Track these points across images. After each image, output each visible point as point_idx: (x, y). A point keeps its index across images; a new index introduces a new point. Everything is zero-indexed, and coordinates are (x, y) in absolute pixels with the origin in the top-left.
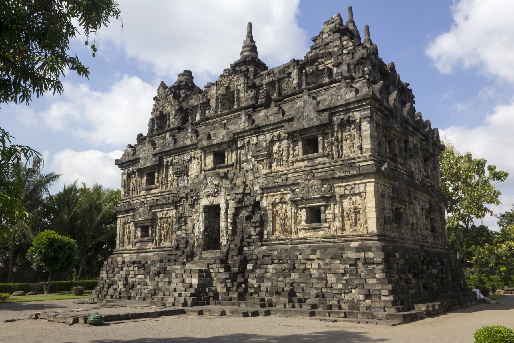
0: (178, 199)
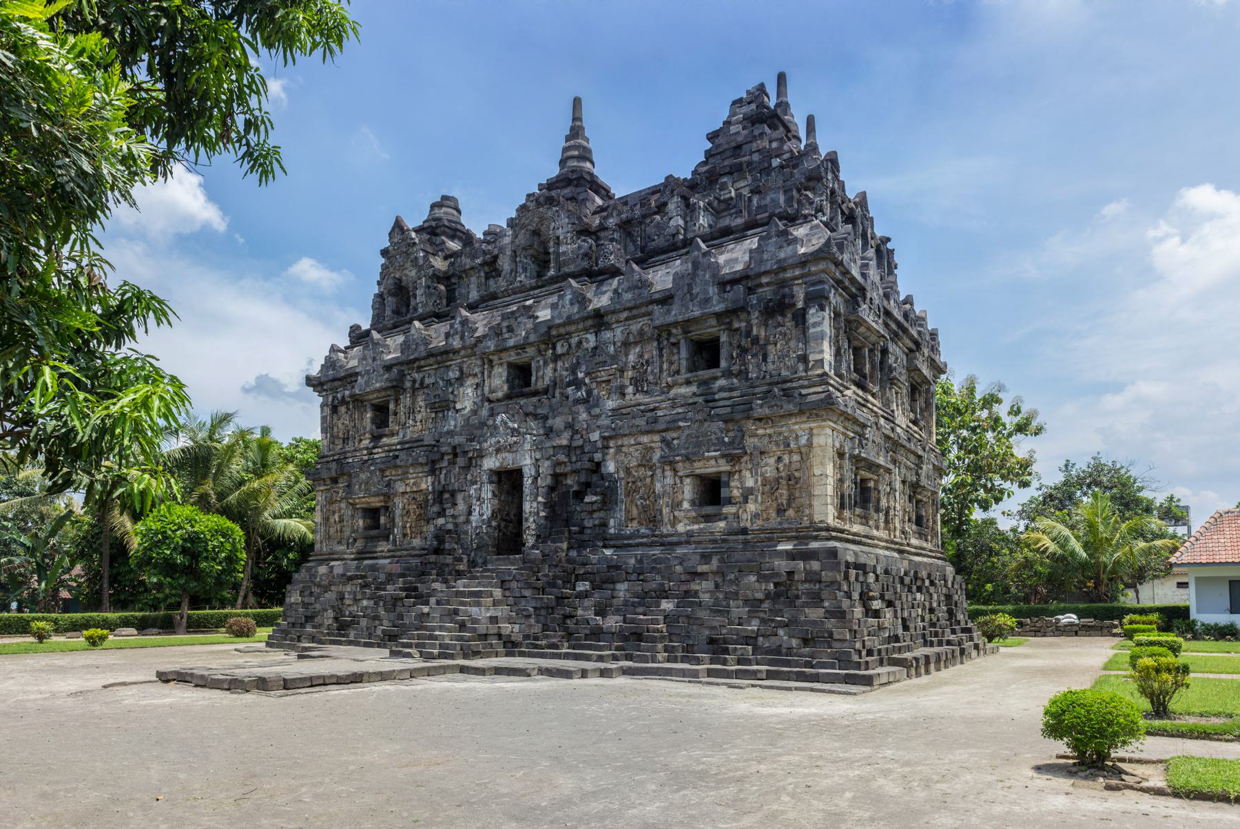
0: (437, 457)
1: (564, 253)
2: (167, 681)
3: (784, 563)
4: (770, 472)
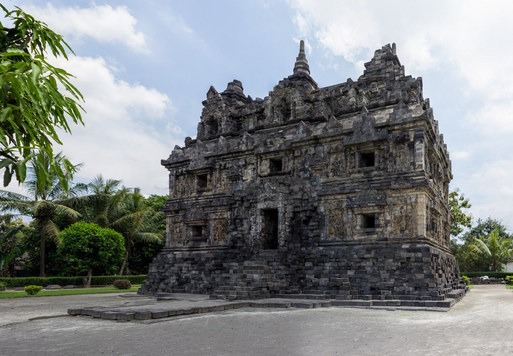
0: (233, 202)
1: (298, 110)
2: (75, 315)
3: (406, 254)
4: (397, 213)
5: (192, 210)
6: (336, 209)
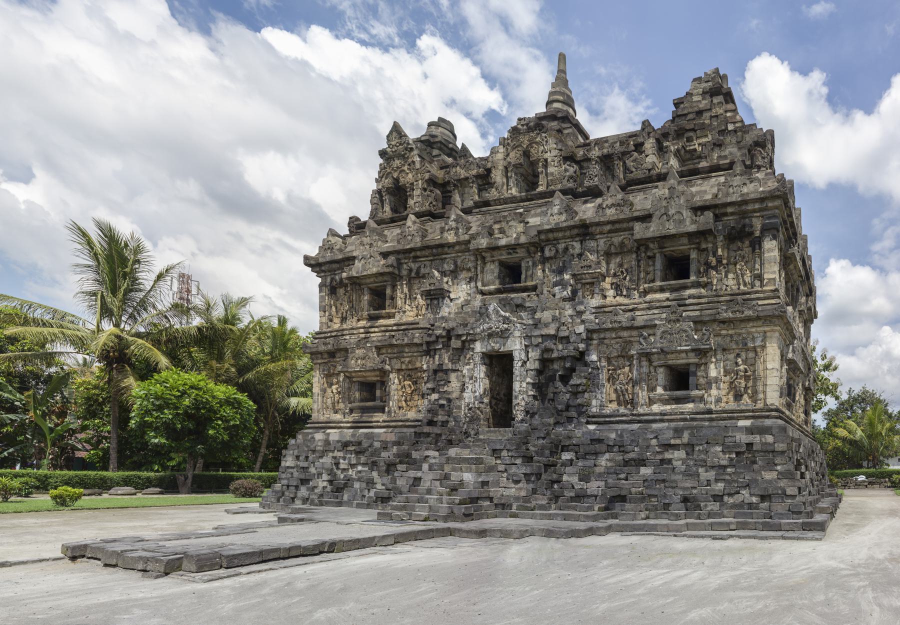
0: (433, 339)
1: (552, 174)
5: (357, 352)
6: (619, 356)
